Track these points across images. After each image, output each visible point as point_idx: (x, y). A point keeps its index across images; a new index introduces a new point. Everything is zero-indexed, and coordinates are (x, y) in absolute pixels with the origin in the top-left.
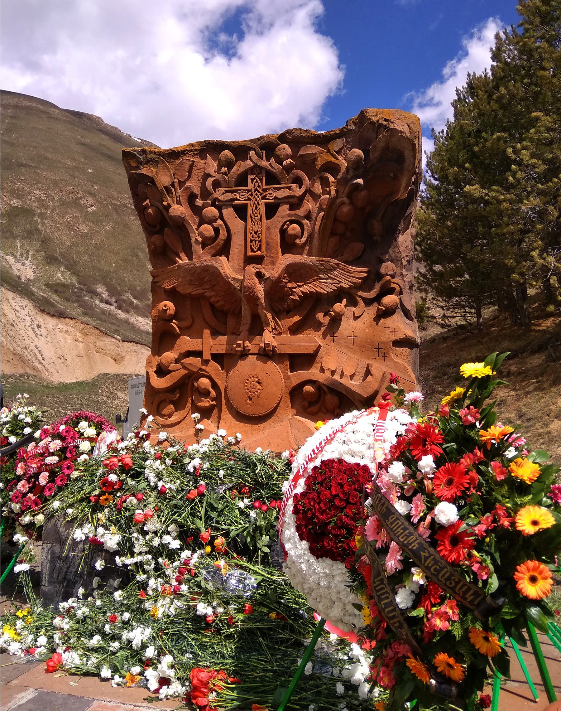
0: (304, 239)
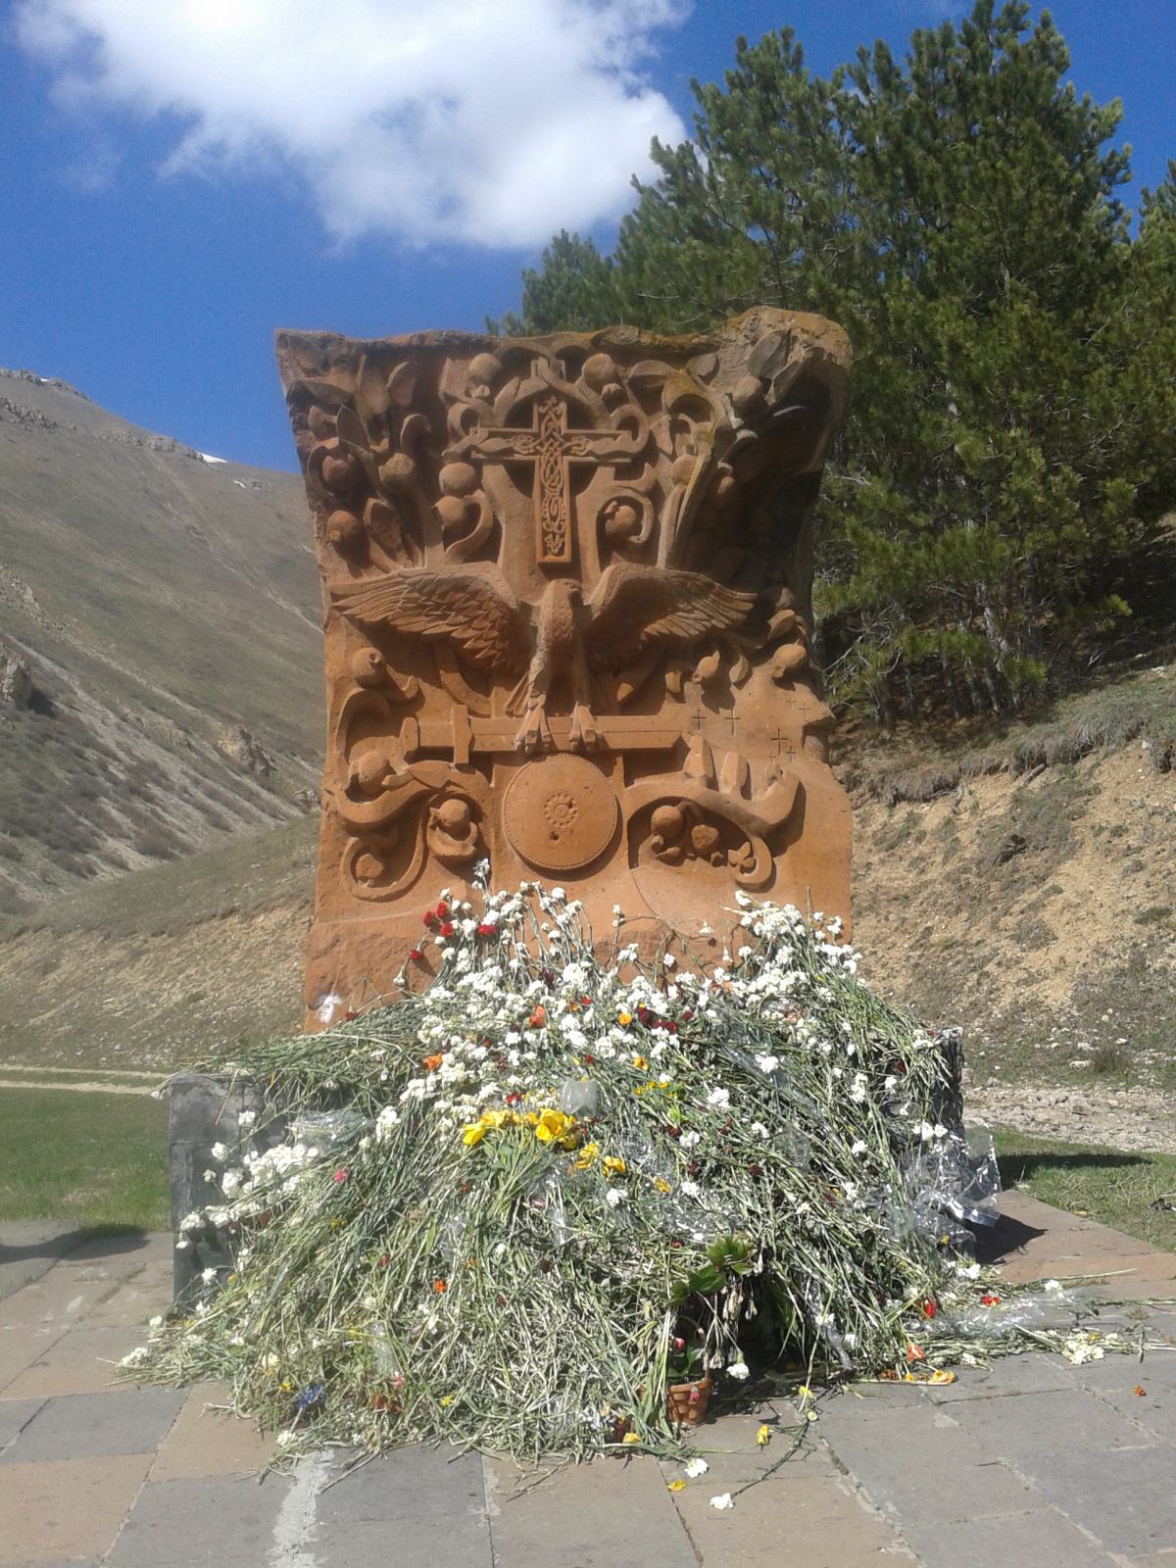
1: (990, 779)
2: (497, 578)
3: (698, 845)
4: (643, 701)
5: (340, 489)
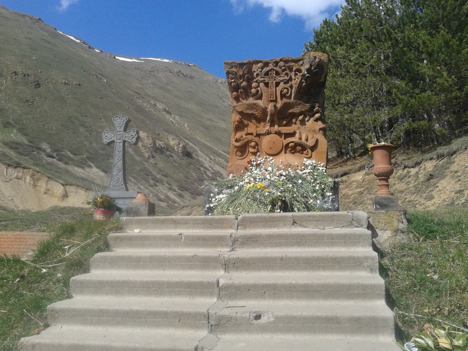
0: (289, 94)
1: (430, 161)
2: (261, 103)
3: (298, 150)
4: (289, 124)
5: (235, 88)
